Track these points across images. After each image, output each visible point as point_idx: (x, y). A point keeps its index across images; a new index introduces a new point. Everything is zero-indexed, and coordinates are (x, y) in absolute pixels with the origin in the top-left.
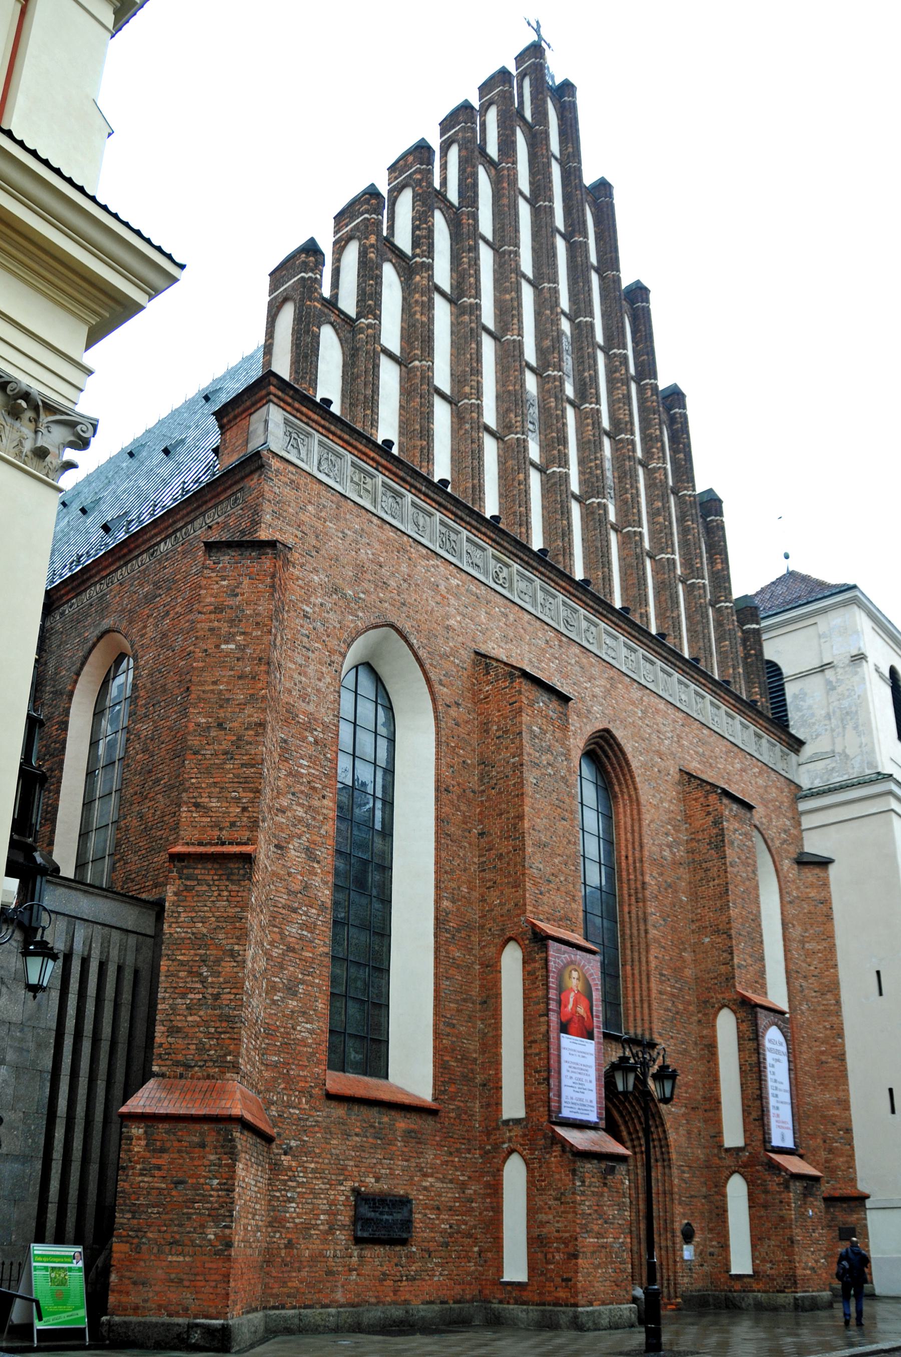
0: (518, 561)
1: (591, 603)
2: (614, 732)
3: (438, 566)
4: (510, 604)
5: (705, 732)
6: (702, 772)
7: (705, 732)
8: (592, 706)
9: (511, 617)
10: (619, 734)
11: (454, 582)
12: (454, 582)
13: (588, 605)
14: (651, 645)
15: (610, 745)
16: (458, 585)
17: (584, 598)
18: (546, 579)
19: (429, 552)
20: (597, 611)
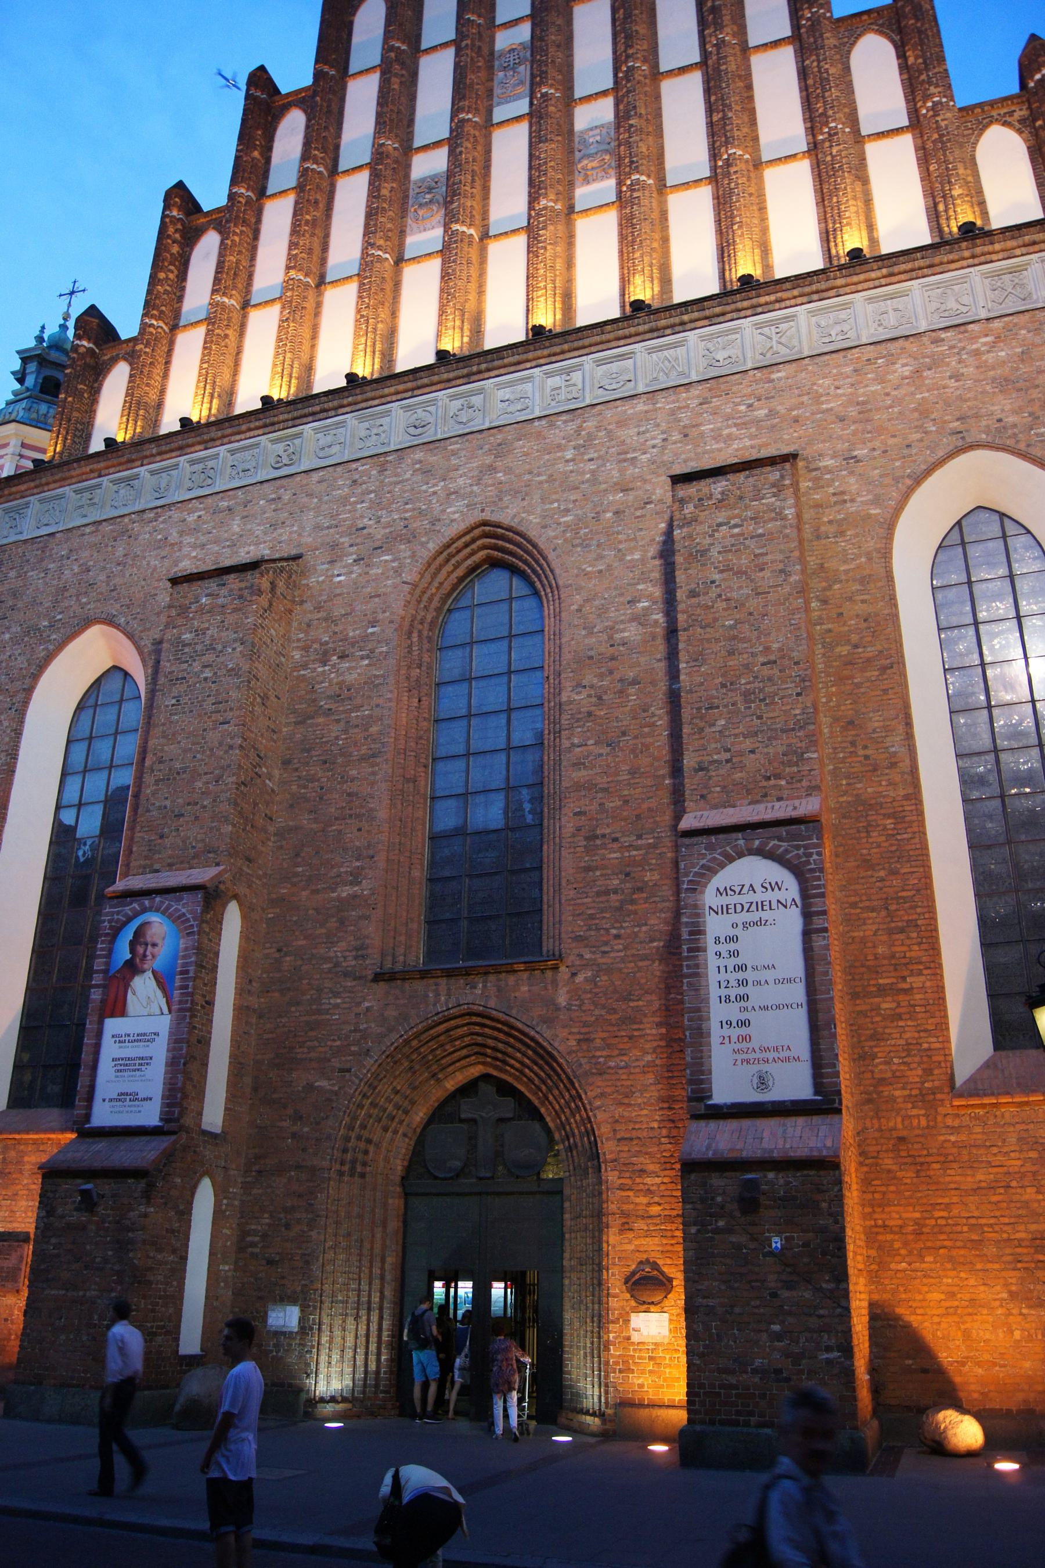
0: (310, 419)
1: (452, 375)
2: (494, 518)
3: (170, 517)
4: (284, 482)
5: (774, 376)
6: (766, 445)
7: (774, 376)
8: (443, 511)
9: (286, 498)
10: (508, 514)
11: (191, 518)
12: (191, 518)
13: (449, 380)
14: (604, 337)
15: (502, 538)
16: (200, 517)
17: (436, 378)
18: (364, 405)
19: (159, 510)
20: (468, 375)
